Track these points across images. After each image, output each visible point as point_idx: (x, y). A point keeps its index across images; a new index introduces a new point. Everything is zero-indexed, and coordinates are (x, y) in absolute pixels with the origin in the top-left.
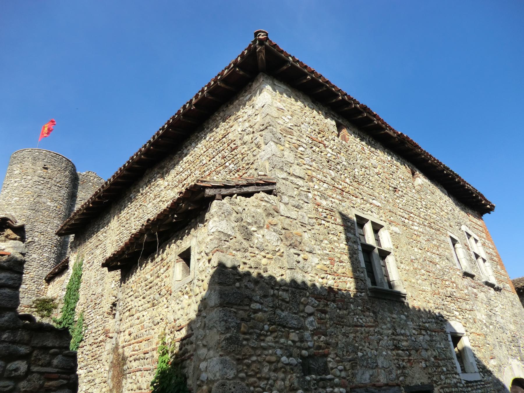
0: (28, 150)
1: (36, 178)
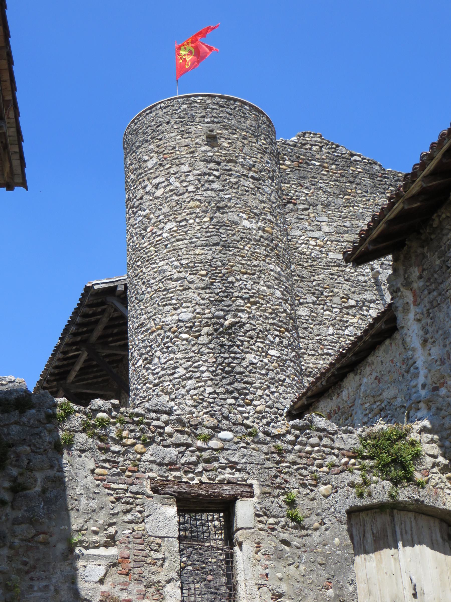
0: (163, 105)
1: (201, 167)
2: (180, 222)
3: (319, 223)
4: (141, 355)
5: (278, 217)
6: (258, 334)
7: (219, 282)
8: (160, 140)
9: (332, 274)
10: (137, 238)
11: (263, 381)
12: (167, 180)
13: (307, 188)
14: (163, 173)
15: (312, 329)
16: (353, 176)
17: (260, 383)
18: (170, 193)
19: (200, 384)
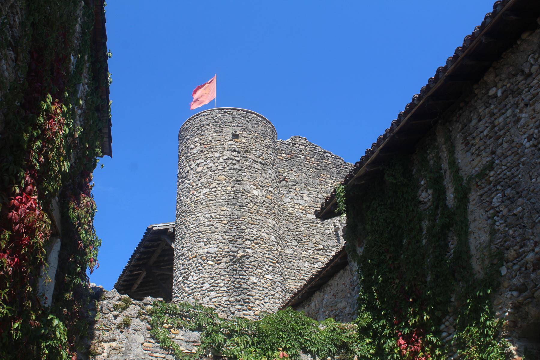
0: (205, 113)
1: (228, 154)
2: (212, 189)
3: (302, 195)
4: (181, 274)
5: (275, 189)
6: (259, 263)
7: (235, 229)
8: (202, 135)
9: (308, 228)
10: (184, 198)
11: (260, 295)
12: (205, 161)
13: (295, 172)
14: (203, 157)
15: (294, 262)
16: (325, 166)
17: (259, 296)
18: (206, 170)
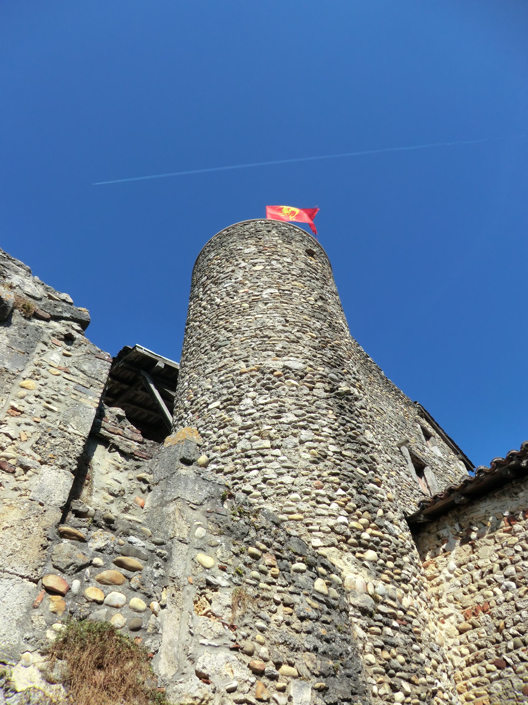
19: (317, 437)
